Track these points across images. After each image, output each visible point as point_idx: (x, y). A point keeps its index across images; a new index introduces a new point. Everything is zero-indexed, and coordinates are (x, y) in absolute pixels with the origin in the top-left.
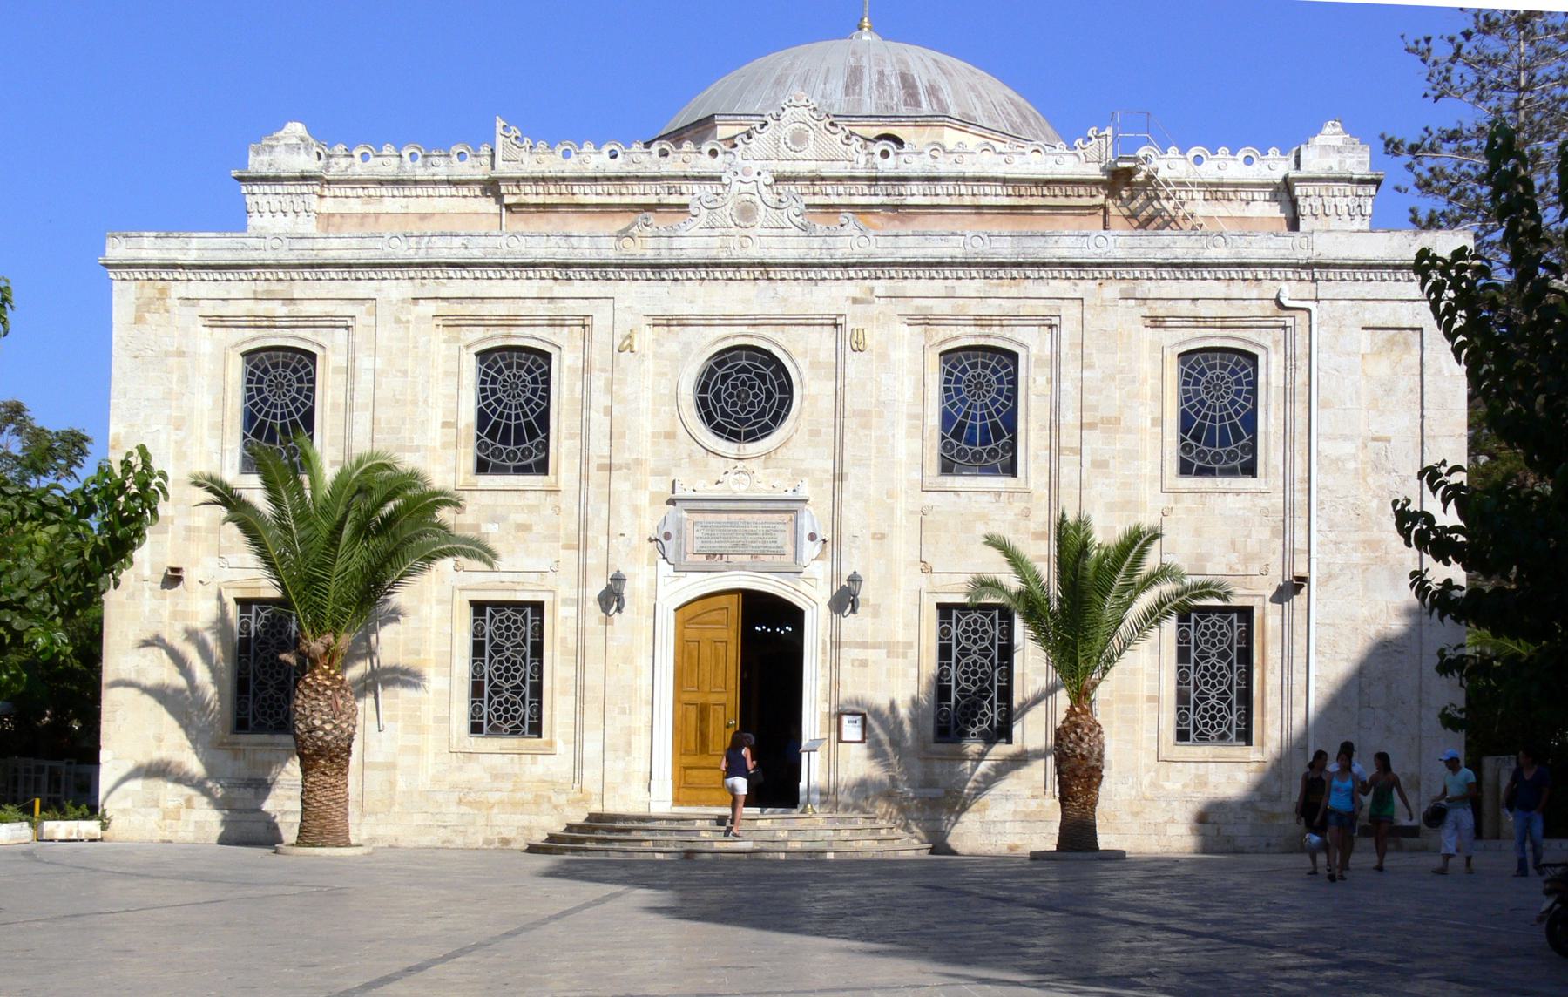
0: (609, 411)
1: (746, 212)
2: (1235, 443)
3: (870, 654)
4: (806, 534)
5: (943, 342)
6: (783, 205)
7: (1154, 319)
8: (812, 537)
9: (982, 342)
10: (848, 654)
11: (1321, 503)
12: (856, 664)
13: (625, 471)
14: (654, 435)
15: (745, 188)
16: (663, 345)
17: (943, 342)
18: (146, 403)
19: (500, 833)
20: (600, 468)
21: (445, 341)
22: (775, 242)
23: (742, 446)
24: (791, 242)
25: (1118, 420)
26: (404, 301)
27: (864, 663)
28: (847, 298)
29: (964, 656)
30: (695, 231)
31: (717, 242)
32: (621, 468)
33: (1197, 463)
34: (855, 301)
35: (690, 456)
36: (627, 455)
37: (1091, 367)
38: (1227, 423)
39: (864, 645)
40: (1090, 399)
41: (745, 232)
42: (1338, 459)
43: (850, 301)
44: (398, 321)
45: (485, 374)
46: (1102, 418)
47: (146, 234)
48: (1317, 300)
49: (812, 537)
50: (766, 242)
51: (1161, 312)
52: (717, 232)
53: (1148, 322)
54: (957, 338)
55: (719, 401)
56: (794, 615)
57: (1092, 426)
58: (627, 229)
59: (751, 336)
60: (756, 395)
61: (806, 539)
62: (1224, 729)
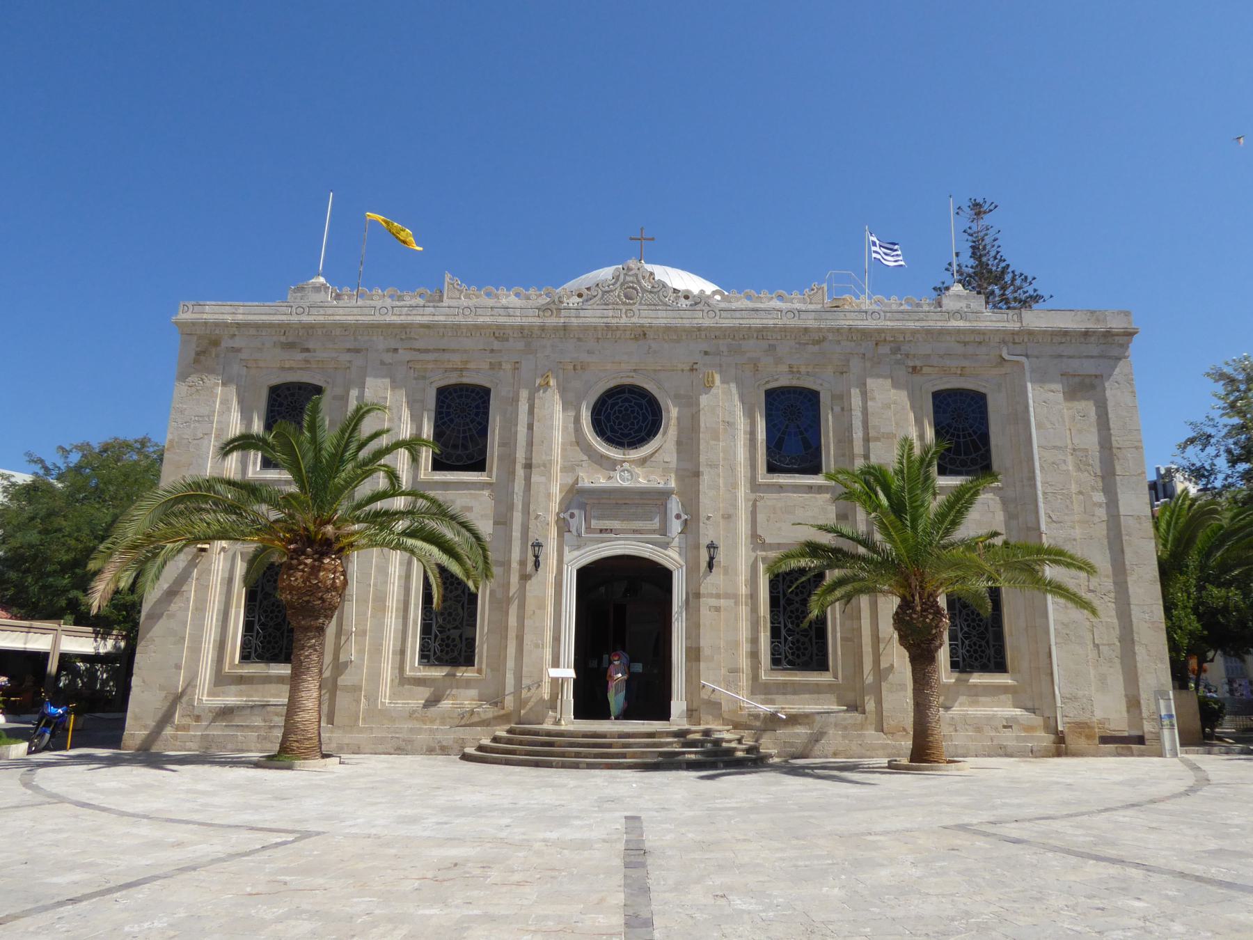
2: (975, 452)
3: (722, 602)
4: (674, 513)
5: (767, 382)
6: (655, 290)
7: (914, 368)
8: (678, 517)
9: (795, 383)
10: (706, 603)
11: (1045, 493)
13: (542, 468)
14: (563, 444)
15: (628, 279)
17: (767, 382)
18: (196, 418)
19: (439, 742)
21: (416, 379)
22: (652, 314)
23: (626, 452)
24: (660, 314)
26: (388, 350)
27: (718, 609)
29: (789, 605)
30: (595, 307)
31: (611, 313)
32: (539, 467)
33: (949, 466)
34: (706, 353)
36: (544, 457)
37: (873, 399)
38: (962, 440)
39: (718, 596)
40: (873, 421)
41: (629, 307)
42: (1053, 463)
44: (382, 363)
45: (443, 402)
47: (208, 303)
48: (1027, 356)
49: (678, 517)
50: (644, 313)
51: (918, 363)
52: (610, 307)
53: (910, 370)
54: (777, 380)
55: (609, 421)
56: (662, 576)
57: (877, 439)
60: (635, 418)
61: (674, 519)
62: (985, 660)
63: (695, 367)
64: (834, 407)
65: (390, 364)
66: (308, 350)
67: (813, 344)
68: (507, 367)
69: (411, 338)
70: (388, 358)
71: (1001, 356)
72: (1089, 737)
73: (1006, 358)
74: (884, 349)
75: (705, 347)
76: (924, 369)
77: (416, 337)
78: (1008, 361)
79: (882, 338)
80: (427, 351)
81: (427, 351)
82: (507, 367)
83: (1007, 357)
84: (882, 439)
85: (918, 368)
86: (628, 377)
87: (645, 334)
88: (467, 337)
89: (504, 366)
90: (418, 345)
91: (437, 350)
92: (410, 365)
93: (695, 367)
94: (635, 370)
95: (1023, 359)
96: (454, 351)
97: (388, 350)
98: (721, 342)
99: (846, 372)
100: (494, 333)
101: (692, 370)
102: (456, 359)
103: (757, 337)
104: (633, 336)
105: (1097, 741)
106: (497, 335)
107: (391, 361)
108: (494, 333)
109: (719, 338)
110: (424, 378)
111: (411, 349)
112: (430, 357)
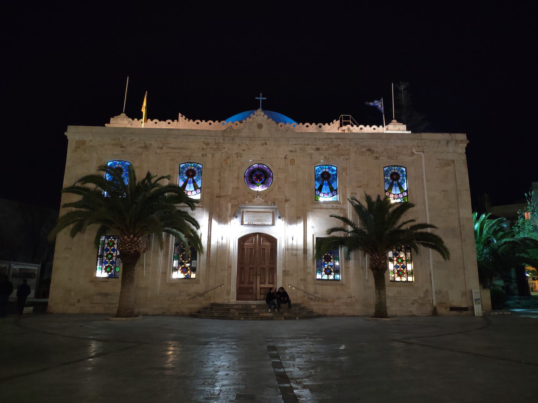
0: (219, 181)
1: (260, 126)
11: (429, 209)
12: (293, 255)
13: (224, 198)
16: (235, 163)
20: (217, 197)
21: (170, 160)
25: (368, 185)
28: (288, 151)
34: (291, 151)
35: (243, 194)
43: (289, 152)
44: (156, 153)
46: (363, 185)
48: (423, 152)
51: (378, 155)
58: (226, 130)
59: (261, 161)
63: (286, 157)
64: (343, 174)
65: (159, 154)
66: (123, 147)
67: (335, 148)
68: (209, 156)
69: (168, 143)
70: (158, 151)
71: (412, 152)
72: (446, 308)
73: (415, 153)
74: (364, 149)
75: (290, 148)
76: (381, 158)
77: (171, 142)
78: (415, 154)
79: (364, 145)
80: (175, 148)
81: (175, 148)
82: (209, 156)
83: (415, 152)
84: (362, 187)
85: (378, 157)
86: (259, 161)
87: (266, 143)
88: (192, 142)
89: (208, 155)
90: (170, 146)
91: (179, 148)
92: (168, 154)
93: (286, 157)
94: (262, 158)
95: (421, 153)
96: (187, 149)
97: (158, 148)
98: (297, 146)
99: (348, 159)
100: (203, 142)
101: (285, 158)
102: (188, 153)
103: (312, 145)
104: (261, 144)
105: (449, 309)
106: (205, 142)
107: (159, 153)
108: (203, 142)
109: (297, 145)
110: (174, 160)
111: (168, 147)
112: (177, 151)
